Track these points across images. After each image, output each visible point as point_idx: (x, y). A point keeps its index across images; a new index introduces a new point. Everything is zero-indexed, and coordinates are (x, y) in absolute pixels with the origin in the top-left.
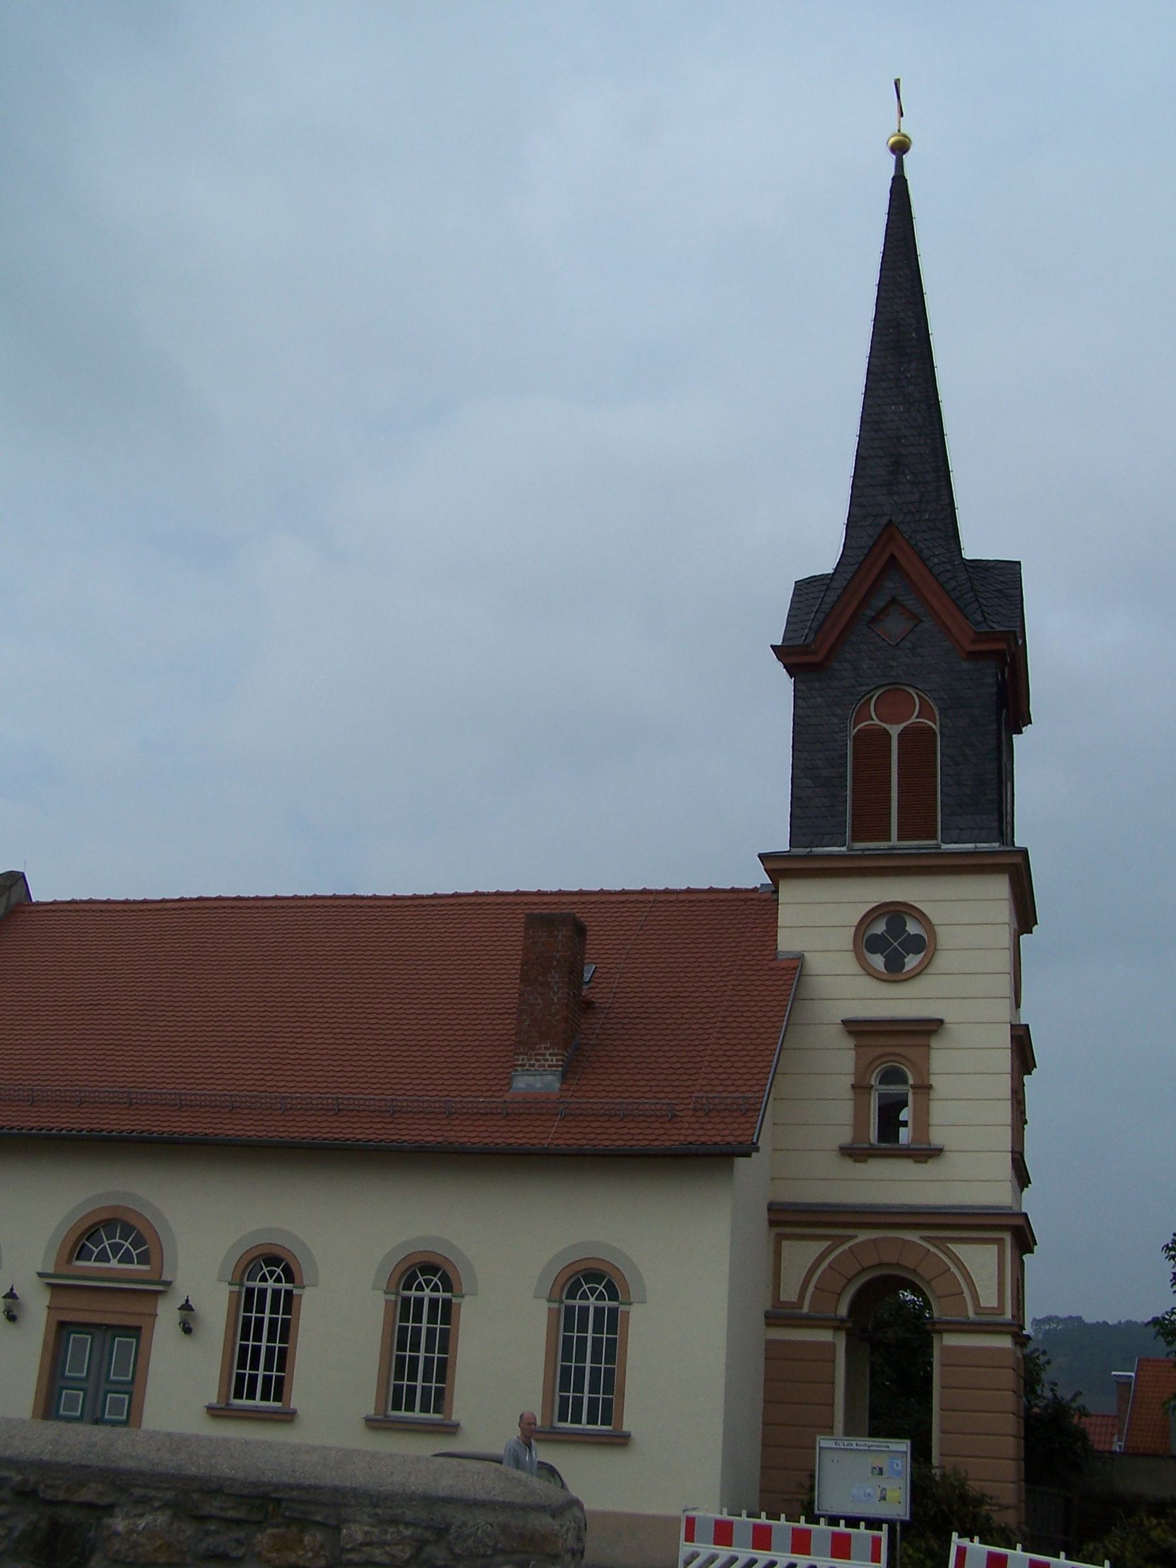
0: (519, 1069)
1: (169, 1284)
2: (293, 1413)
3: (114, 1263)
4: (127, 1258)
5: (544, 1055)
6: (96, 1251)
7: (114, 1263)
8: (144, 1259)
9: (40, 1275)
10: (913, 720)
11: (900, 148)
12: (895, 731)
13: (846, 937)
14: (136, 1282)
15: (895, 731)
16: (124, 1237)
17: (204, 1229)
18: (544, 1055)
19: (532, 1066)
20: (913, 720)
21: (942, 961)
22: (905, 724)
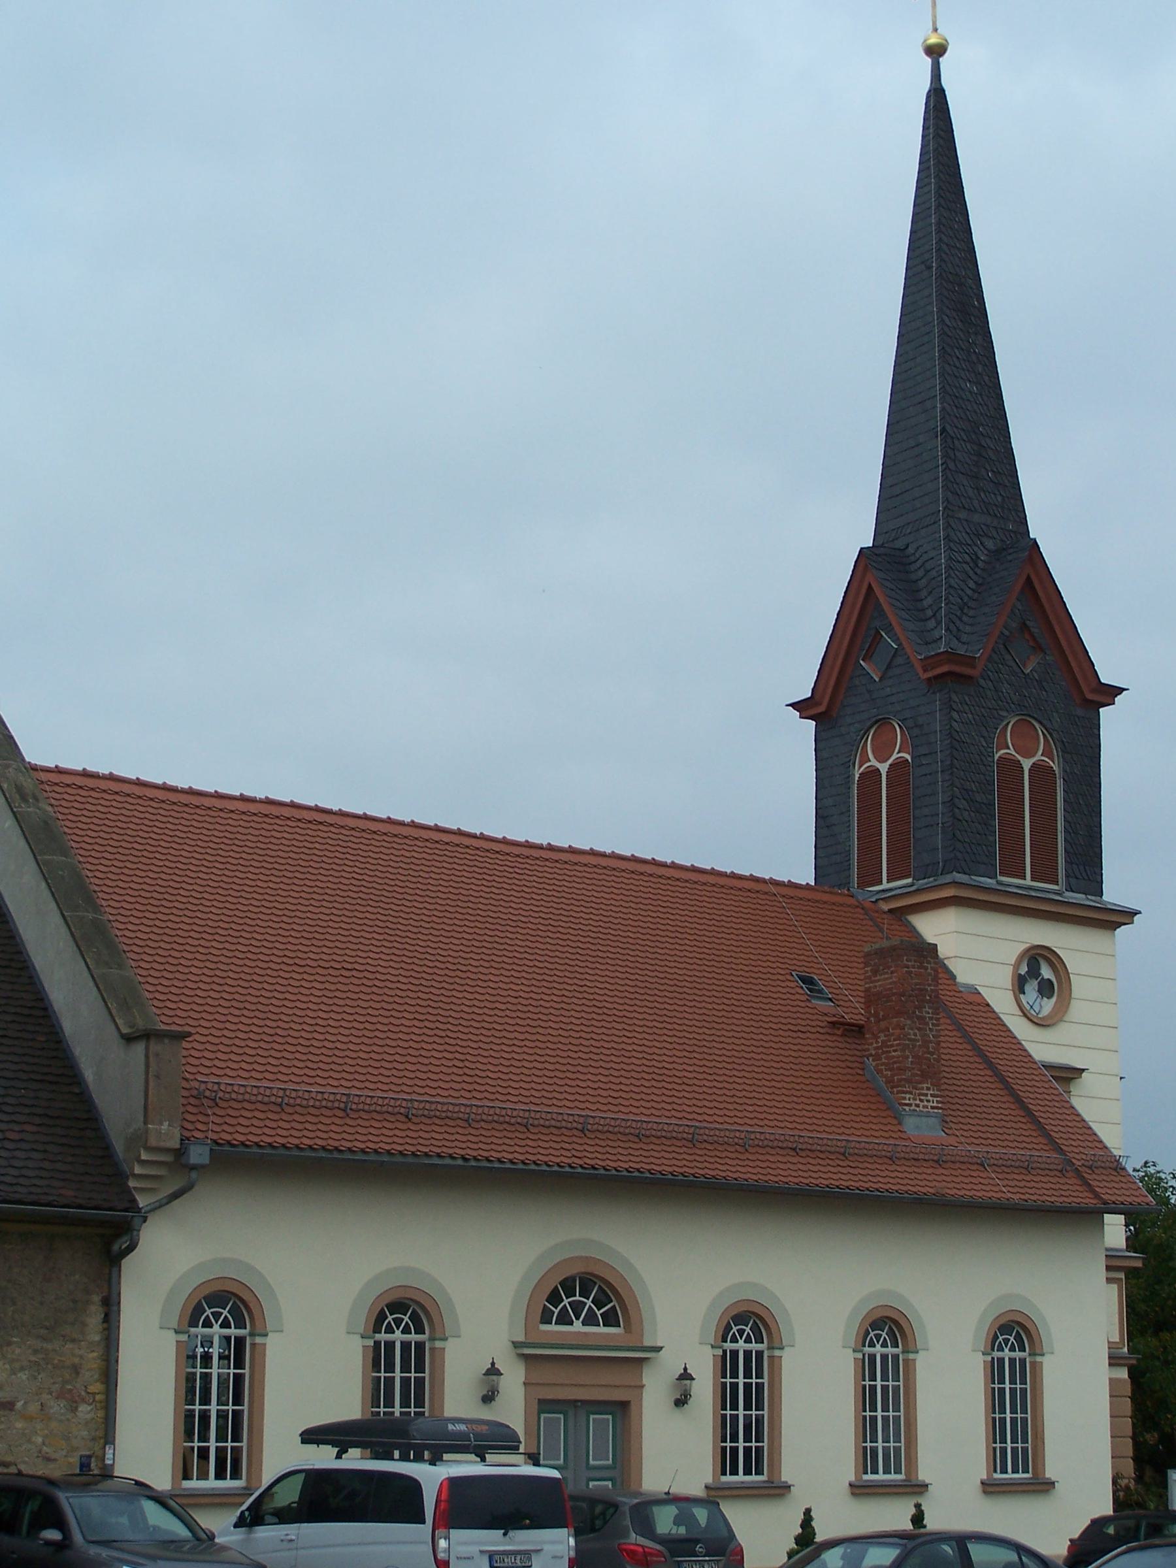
0: (907, 1108)
1: (660, 1349)
2: (787, 1487)
3: (578, 1326)
4: (590, 1320)
5: (926, 1095)
6: (556, 1311)
7: (578, 1326)
8: (610, 1319)
9: (516, 1345)
10: (1039, 756)
11: (936, 52)
12: (1027, 764)
13: (1005, 977)
14: (552, 1346)
15: (1027, 764)
16: (585, 1293)
17: (680, 1281)
18: (926, 1095)
19: (917, 1106)
20: (1039, 756)
21: (1077, 1010)
22: (1020, 758)
